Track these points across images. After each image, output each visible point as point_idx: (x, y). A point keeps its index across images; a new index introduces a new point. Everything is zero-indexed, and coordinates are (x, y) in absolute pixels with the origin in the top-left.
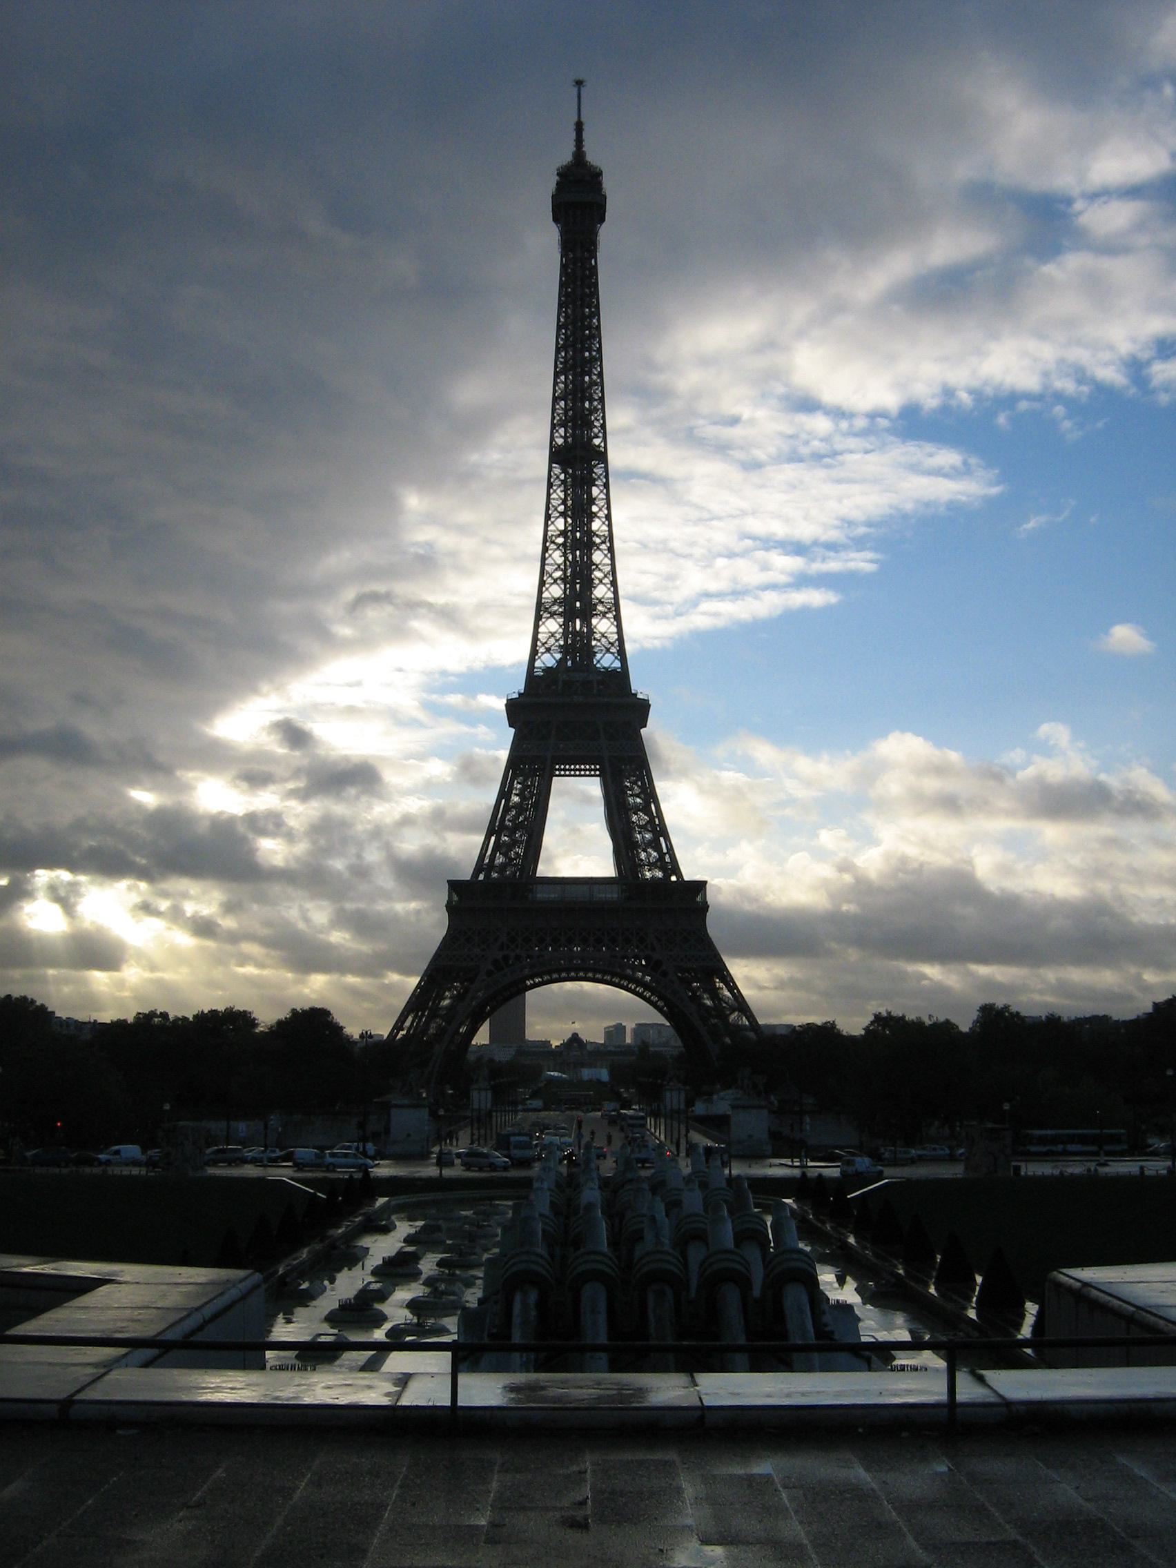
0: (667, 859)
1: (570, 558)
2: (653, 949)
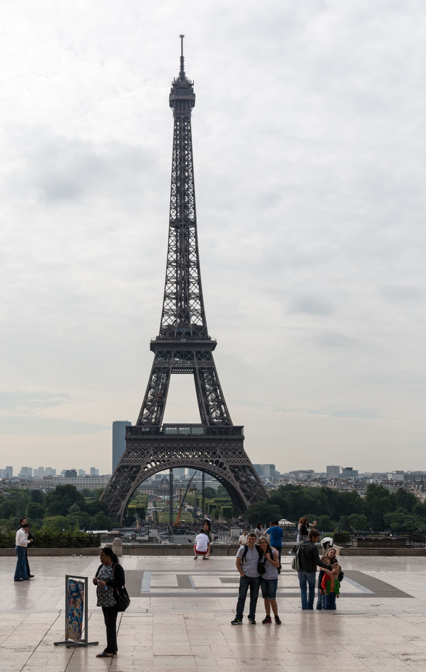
0: (225, 415)
1: (179, 272)
2: (219, 457)
